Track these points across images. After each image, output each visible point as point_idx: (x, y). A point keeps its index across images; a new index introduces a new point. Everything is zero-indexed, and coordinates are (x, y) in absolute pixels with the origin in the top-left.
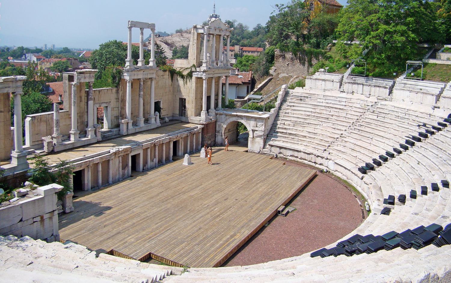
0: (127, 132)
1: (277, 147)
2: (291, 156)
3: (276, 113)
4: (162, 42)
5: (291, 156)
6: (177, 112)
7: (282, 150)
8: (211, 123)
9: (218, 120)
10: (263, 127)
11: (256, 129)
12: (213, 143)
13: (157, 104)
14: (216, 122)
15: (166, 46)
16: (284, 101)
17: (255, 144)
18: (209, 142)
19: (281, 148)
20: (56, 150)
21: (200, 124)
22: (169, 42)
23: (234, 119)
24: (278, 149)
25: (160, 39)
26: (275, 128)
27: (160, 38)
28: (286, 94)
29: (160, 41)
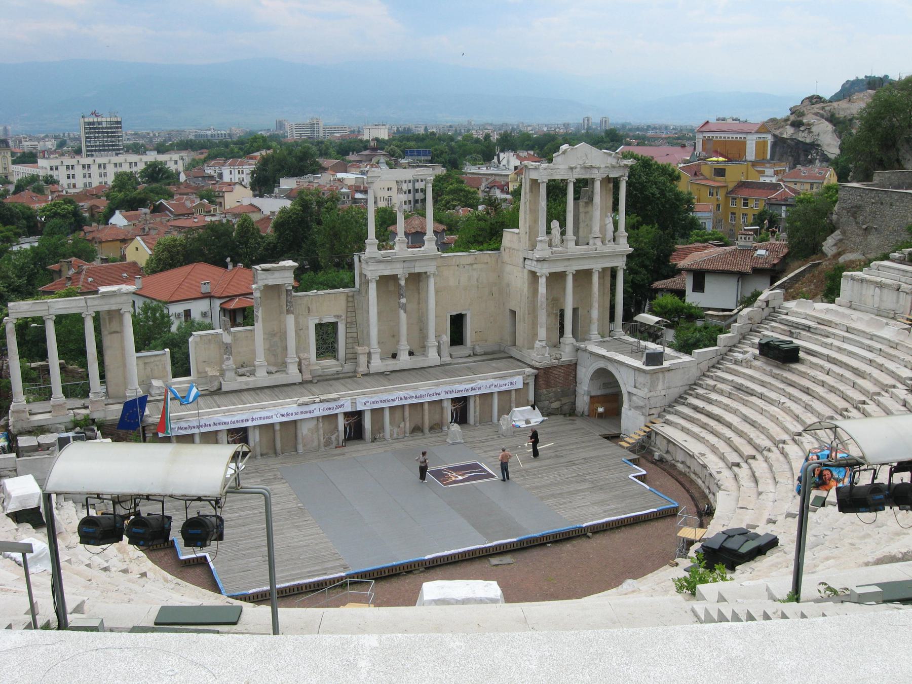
0: (366, 369)
1: (665, 438)
2: (683, 463)
3: (715, 361)
4: (822, 116)
6: (508, 338)
8: (555, 367)
9: (579, 362)
11: (634, 391)
12: (566, 408)
13: (457, 322)
14: (576, 364)
15: (829, 127)
17: (633, 423)
18: (556, 405)
19: (669, 441)
20: (224, 389)
21: (532, 367)
22: (841, 115)
23: (601, 364)
25: (817, 108)
27: (818, 106)
29: (816, 114)
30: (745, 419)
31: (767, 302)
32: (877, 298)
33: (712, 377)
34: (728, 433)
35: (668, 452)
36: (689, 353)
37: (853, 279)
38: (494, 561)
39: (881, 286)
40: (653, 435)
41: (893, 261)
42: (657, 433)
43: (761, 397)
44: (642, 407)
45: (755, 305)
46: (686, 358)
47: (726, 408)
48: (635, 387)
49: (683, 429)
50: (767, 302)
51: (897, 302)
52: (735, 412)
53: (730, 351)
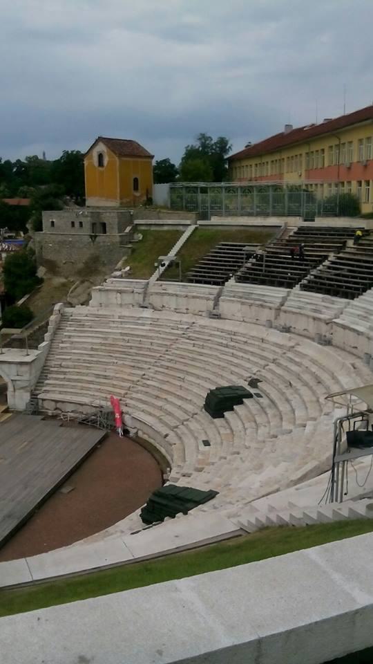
2: (72, 412)
5: (72, 412)
7: (59, 405)
10: (28, 375)
16: (58, 328)
19: (57, 402)
24: (53, 403)
26: (47, 373)
28: (63, 318)
30: (98, 376)
31: (59, 311)
32: (119, 299)
33: (53, 360)
34: (91, 386)
35: (56, 409)
36: (36, 348)
37: (100, 290)
38: (65, 490)
39: (120, 292)
40: (40, 402)
41: (115, 277)
42: (43, 400)
43: (97, 362)
44: (27, 387)
45: (54, 313)
46: (37, 352)
47: (78, 373)
48: (18, 375)
49: (60, 393)
50: (59, 311)
51: (134, 298)
52: (87, 375)
53: (52, 343)
